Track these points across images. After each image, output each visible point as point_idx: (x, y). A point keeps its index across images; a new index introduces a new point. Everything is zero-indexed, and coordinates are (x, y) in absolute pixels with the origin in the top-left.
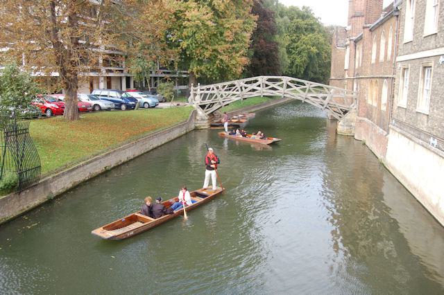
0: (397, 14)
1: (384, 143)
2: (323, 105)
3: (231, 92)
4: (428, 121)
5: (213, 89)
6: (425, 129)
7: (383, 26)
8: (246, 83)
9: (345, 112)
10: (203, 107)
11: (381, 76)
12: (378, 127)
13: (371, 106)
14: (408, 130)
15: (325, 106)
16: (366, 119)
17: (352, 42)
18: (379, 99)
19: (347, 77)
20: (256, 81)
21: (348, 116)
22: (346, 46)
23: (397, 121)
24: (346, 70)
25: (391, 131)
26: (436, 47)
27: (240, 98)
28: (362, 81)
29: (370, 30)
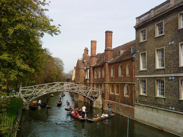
0: (134, 59)
1: (132, 112)
2: (87, 95)
3: (42, 90)
4: (165, 100)
5: (29, 88)
6: (163, 104)
7: (120, 63)
8: (49, 85)
9: (96, 98)
10: (26, 98)
11: (122, 83)
12: (123, 104)
13: (114, 96)
14: (151, 104)
15: (88, 96)
16: (110, 101)
17: (92, 67)
18: (122, 93)
19: (88, 82)
20: (55, 84)
21: (98, 100)
22: (87, 69)
23: (140, 101)
24: (87, 79)
25: (136, 106)
26: (165, 74)
27: (47, 93)
28: (106, 84)
29: (109, 64)
